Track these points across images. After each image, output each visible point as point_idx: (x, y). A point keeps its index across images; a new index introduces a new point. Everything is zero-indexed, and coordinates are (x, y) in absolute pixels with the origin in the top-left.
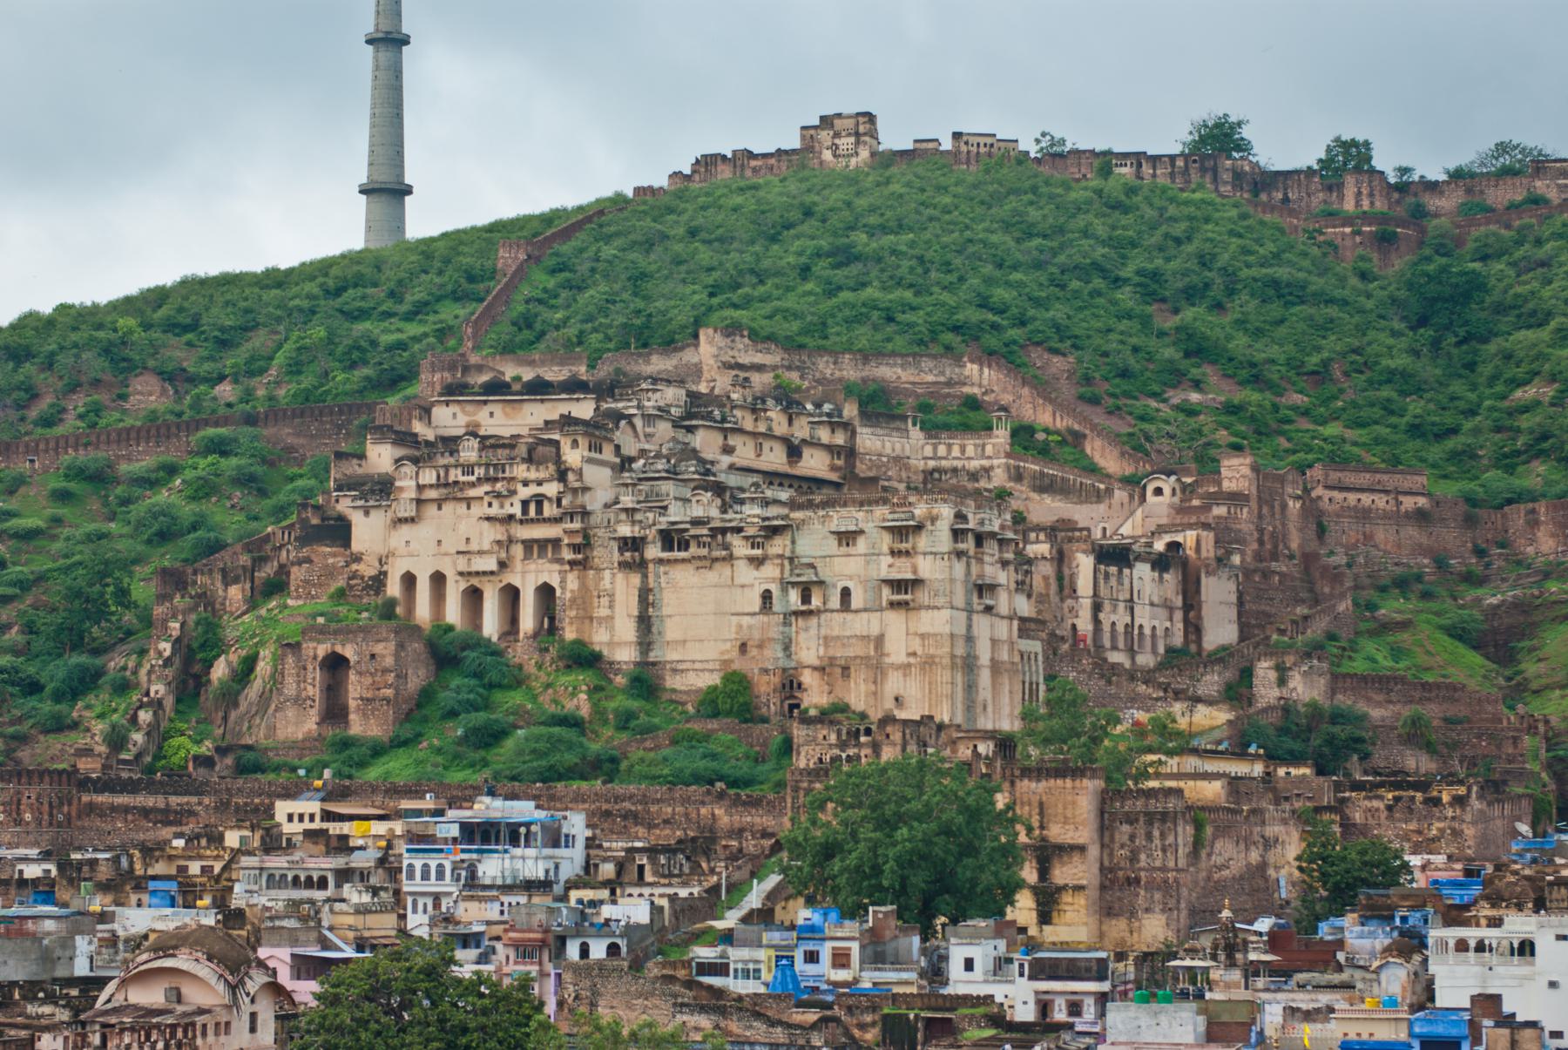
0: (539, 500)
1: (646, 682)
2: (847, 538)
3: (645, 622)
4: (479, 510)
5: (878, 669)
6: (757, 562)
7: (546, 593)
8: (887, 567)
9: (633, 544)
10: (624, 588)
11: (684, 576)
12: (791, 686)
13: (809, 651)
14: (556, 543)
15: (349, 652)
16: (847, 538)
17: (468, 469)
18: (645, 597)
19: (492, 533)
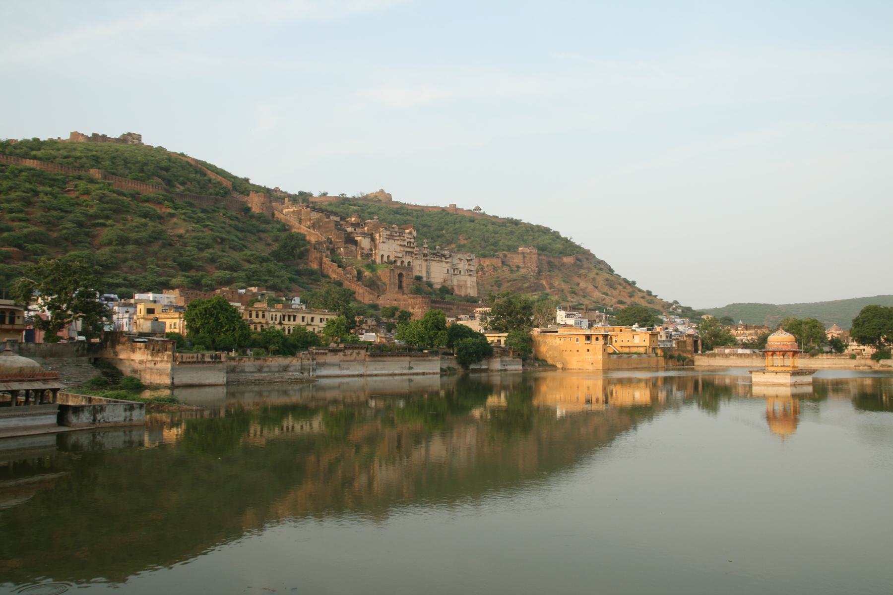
0: (410, 242)
1: (430, 285)
2: (461, 260)
3: (428, 272)
4: (399, 242)
5: (466, 288)
6: (447, 262)
7: (409, 263)
8: (466, 267)
9: (425, 255)
10: (424, 264)
11: (434, 263)
12: (453, 289)
13: (455, 283)
14: (412, 252)
15: (404, 273)
16: (461, 260)
17: (396, 232)
18: (428, 268)
19: (399, 249)
